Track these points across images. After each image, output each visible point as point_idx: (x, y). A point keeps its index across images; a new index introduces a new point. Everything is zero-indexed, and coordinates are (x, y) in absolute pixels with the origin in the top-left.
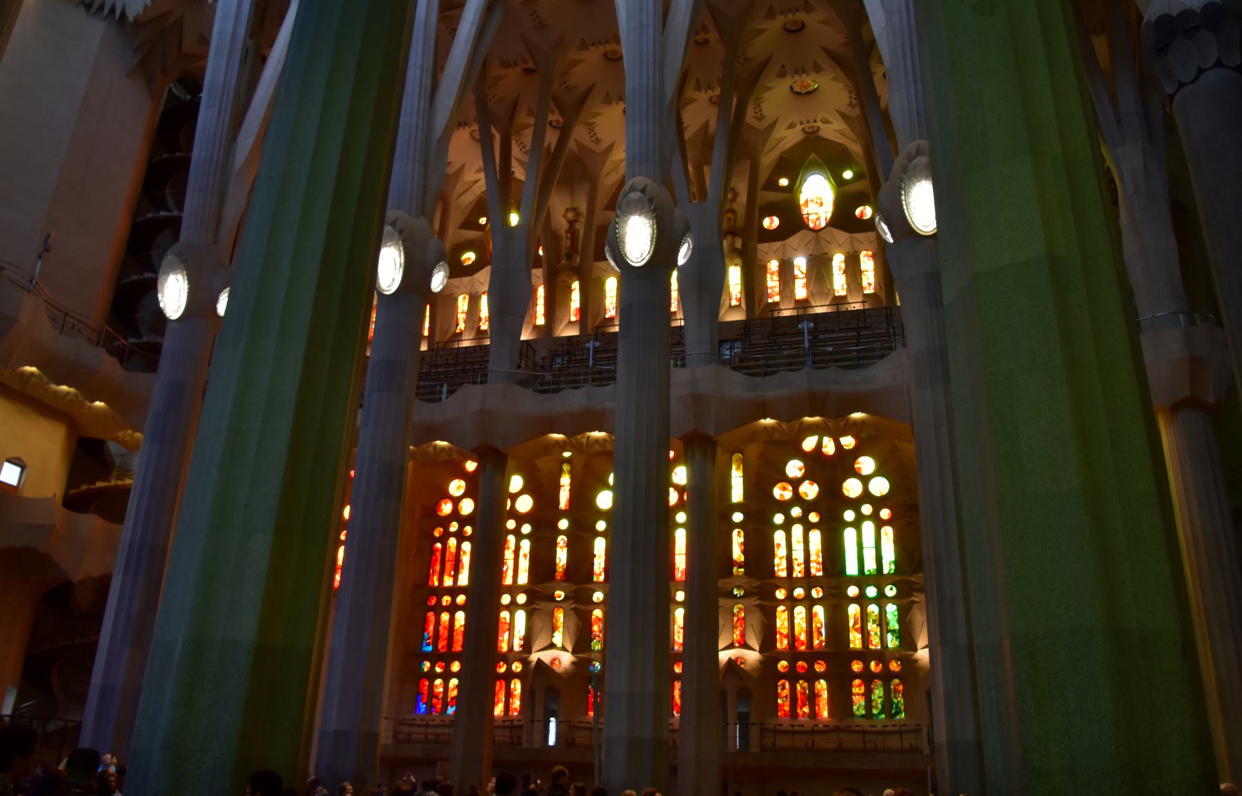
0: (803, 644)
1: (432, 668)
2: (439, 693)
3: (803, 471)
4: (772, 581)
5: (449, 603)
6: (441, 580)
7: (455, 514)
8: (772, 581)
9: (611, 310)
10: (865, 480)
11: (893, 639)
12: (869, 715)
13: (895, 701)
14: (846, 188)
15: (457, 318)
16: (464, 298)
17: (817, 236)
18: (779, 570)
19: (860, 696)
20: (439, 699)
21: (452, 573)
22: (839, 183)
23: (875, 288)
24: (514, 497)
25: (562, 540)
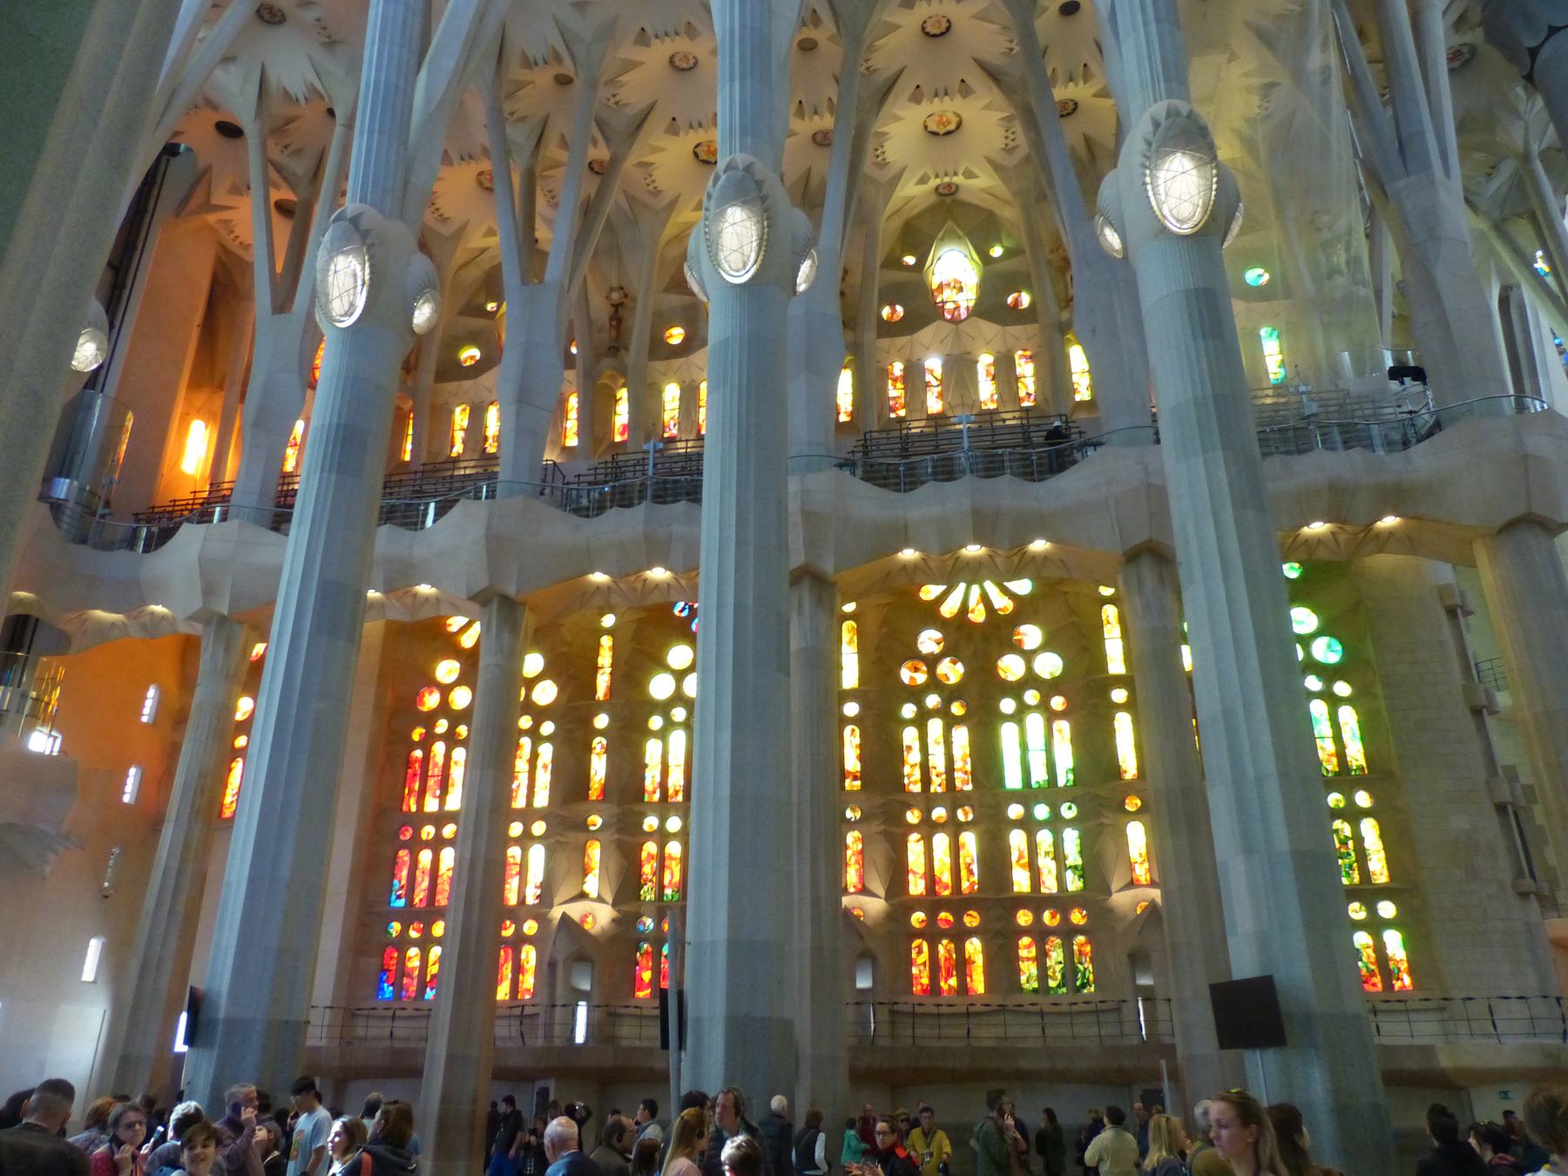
0: (946, 887)
1: (405, 930)
2: (413, 969)
3: (942, 644)
4: (900, 797)
5: (431, 837)
6: (420, 803)
7: (444, 709)
8: (900, 797)
9: (672, 427)
10: (1029, 656)
11: (1074, 879)
12: (1043, 988)
13: (1081, 967)
14: (998, 267)
15: (453, 437)
16: (464, 410)
17: (957, 330)
18: (910, 783)
19: (1030, 963)
20: (412, 978)
21: (438, 793)
22: (986, 259)
23: (1035, 400)
24: (531, 684)
25: (599, 743)
